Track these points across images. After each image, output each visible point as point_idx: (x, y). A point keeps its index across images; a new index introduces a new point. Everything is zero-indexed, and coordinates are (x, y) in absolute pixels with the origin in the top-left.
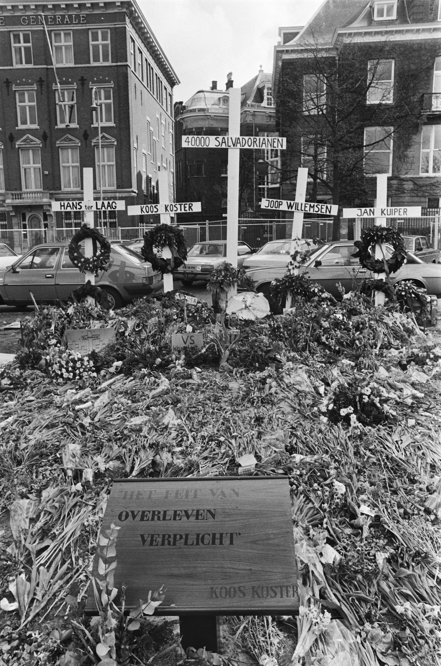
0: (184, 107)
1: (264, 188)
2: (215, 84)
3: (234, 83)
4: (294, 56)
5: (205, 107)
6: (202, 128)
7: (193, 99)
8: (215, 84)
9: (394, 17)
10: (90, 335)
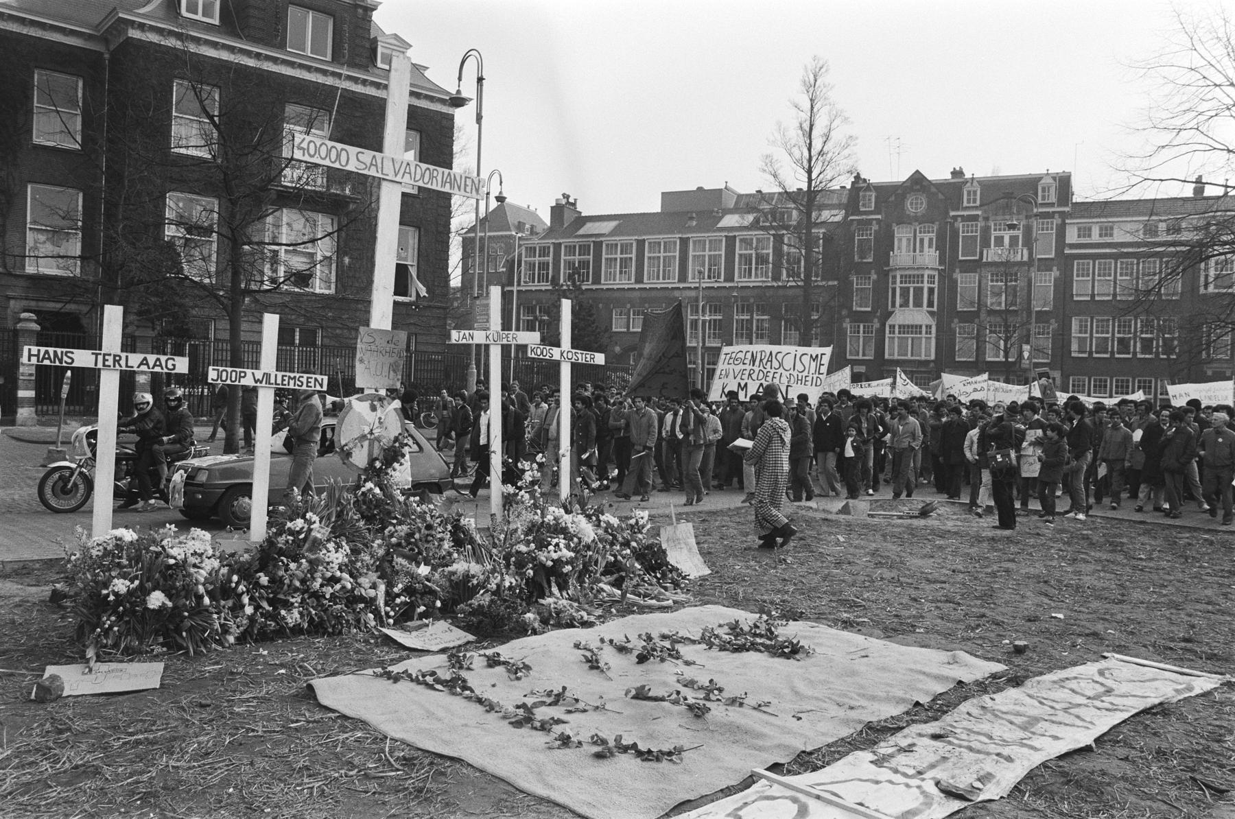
9: (216, 21)
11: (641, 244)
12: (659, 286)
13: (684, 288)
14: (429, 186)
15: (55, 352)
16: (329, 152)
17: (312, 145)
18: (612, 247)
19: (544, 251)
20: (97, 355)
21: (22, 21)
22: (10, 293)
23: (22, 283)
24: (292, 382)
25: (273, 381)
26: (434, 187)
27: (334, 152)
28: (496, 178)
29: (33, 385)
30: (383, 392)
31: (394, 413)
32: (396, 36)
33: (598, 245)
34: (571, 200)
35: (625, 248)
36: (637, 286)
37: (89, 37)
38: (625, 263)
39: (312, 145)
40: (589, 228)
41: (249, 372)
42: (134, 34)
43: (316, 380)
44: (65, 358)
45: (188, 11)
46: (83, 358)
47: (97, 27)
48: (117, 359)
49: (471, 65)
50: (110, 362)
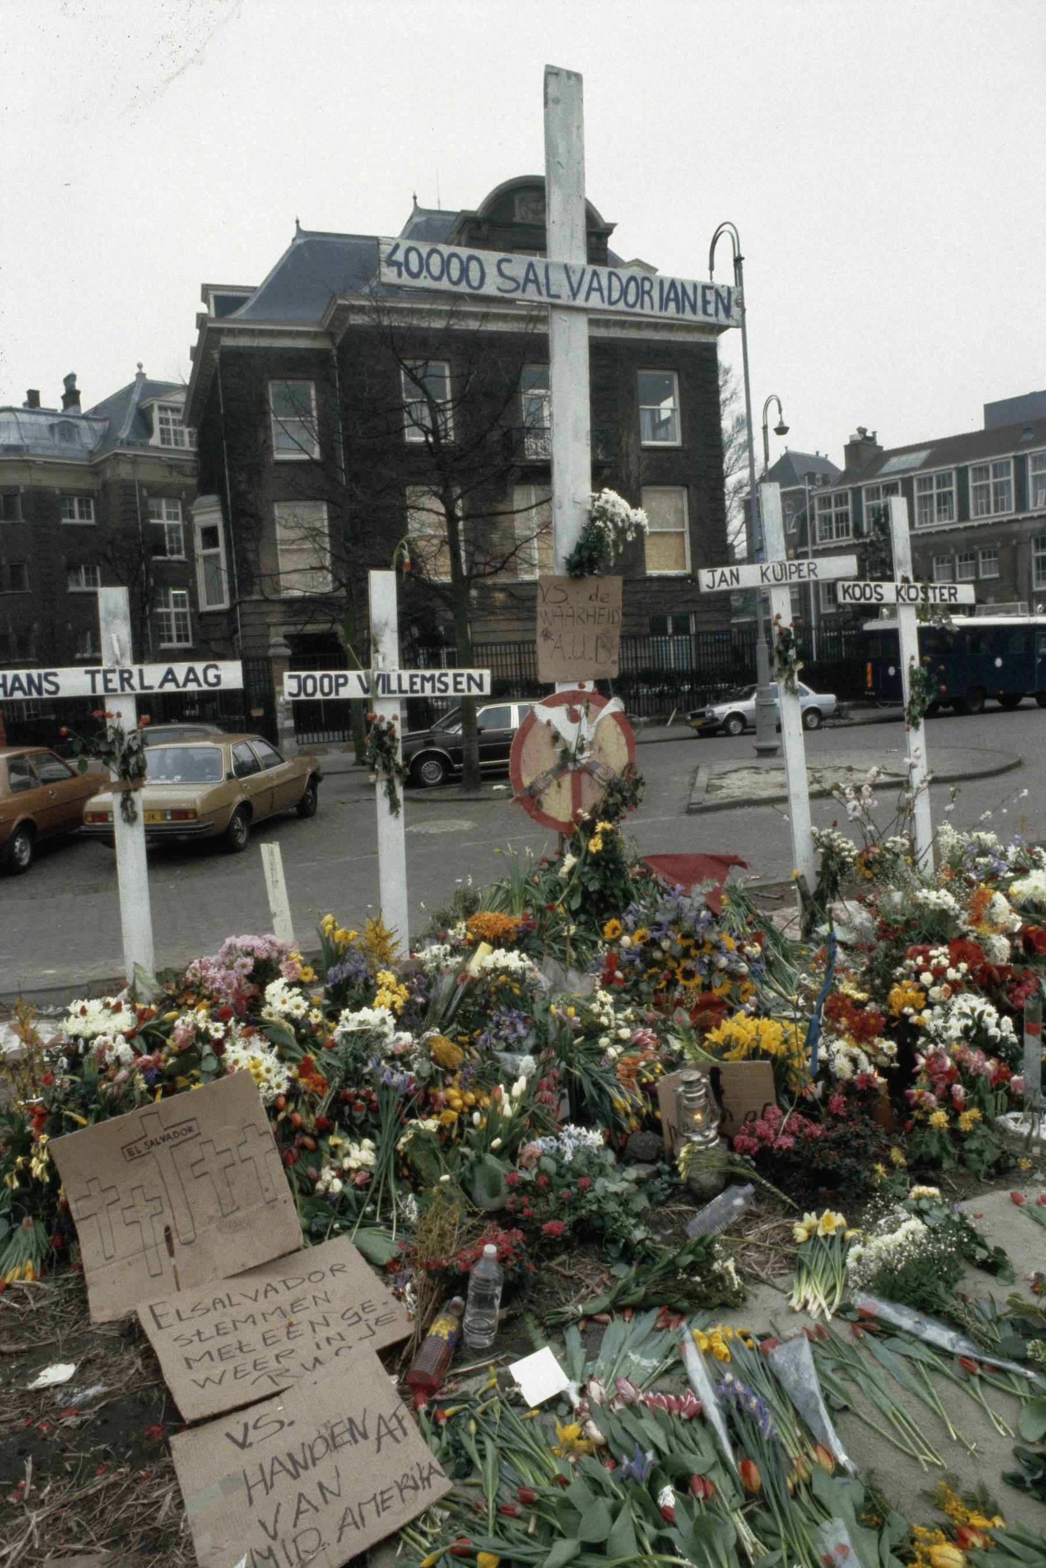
1: (168, 615)
2: (33, 396)
3: (82, 397)
4: (244, 342)
5: (20, 443)
6: (17, 487)
8: (33, 396)
11: (962, 473)
12: (990, 521)
13: (1024, 519)
14: (637, 309)
15: (29, 677)
16: (446, 265)
17: (413, 256)
18: (925, 483)
19: (841, 499)
20: (93, 673)
21: (252, 333)
24: (428, 686)
25: (394, 686)
26: (647, 310)
27: (455, 265)
28: (773, 406)
29: (290, 714)
30: (590, 687)
31: (612, 722)
32: (638, 263)
34: (869, 434)
35: (943, 480)
36: (961, 525)
37: (315, 335)
38: (944, 499)
39: (413, 256)
40: (895, 464)
41: (352, 675)
43: (470, 678)
44: (46, 685)
46: (72, 681)
47: (320, 323)
48: (125, 680)
49: (725, 242)
50: (115, 684)
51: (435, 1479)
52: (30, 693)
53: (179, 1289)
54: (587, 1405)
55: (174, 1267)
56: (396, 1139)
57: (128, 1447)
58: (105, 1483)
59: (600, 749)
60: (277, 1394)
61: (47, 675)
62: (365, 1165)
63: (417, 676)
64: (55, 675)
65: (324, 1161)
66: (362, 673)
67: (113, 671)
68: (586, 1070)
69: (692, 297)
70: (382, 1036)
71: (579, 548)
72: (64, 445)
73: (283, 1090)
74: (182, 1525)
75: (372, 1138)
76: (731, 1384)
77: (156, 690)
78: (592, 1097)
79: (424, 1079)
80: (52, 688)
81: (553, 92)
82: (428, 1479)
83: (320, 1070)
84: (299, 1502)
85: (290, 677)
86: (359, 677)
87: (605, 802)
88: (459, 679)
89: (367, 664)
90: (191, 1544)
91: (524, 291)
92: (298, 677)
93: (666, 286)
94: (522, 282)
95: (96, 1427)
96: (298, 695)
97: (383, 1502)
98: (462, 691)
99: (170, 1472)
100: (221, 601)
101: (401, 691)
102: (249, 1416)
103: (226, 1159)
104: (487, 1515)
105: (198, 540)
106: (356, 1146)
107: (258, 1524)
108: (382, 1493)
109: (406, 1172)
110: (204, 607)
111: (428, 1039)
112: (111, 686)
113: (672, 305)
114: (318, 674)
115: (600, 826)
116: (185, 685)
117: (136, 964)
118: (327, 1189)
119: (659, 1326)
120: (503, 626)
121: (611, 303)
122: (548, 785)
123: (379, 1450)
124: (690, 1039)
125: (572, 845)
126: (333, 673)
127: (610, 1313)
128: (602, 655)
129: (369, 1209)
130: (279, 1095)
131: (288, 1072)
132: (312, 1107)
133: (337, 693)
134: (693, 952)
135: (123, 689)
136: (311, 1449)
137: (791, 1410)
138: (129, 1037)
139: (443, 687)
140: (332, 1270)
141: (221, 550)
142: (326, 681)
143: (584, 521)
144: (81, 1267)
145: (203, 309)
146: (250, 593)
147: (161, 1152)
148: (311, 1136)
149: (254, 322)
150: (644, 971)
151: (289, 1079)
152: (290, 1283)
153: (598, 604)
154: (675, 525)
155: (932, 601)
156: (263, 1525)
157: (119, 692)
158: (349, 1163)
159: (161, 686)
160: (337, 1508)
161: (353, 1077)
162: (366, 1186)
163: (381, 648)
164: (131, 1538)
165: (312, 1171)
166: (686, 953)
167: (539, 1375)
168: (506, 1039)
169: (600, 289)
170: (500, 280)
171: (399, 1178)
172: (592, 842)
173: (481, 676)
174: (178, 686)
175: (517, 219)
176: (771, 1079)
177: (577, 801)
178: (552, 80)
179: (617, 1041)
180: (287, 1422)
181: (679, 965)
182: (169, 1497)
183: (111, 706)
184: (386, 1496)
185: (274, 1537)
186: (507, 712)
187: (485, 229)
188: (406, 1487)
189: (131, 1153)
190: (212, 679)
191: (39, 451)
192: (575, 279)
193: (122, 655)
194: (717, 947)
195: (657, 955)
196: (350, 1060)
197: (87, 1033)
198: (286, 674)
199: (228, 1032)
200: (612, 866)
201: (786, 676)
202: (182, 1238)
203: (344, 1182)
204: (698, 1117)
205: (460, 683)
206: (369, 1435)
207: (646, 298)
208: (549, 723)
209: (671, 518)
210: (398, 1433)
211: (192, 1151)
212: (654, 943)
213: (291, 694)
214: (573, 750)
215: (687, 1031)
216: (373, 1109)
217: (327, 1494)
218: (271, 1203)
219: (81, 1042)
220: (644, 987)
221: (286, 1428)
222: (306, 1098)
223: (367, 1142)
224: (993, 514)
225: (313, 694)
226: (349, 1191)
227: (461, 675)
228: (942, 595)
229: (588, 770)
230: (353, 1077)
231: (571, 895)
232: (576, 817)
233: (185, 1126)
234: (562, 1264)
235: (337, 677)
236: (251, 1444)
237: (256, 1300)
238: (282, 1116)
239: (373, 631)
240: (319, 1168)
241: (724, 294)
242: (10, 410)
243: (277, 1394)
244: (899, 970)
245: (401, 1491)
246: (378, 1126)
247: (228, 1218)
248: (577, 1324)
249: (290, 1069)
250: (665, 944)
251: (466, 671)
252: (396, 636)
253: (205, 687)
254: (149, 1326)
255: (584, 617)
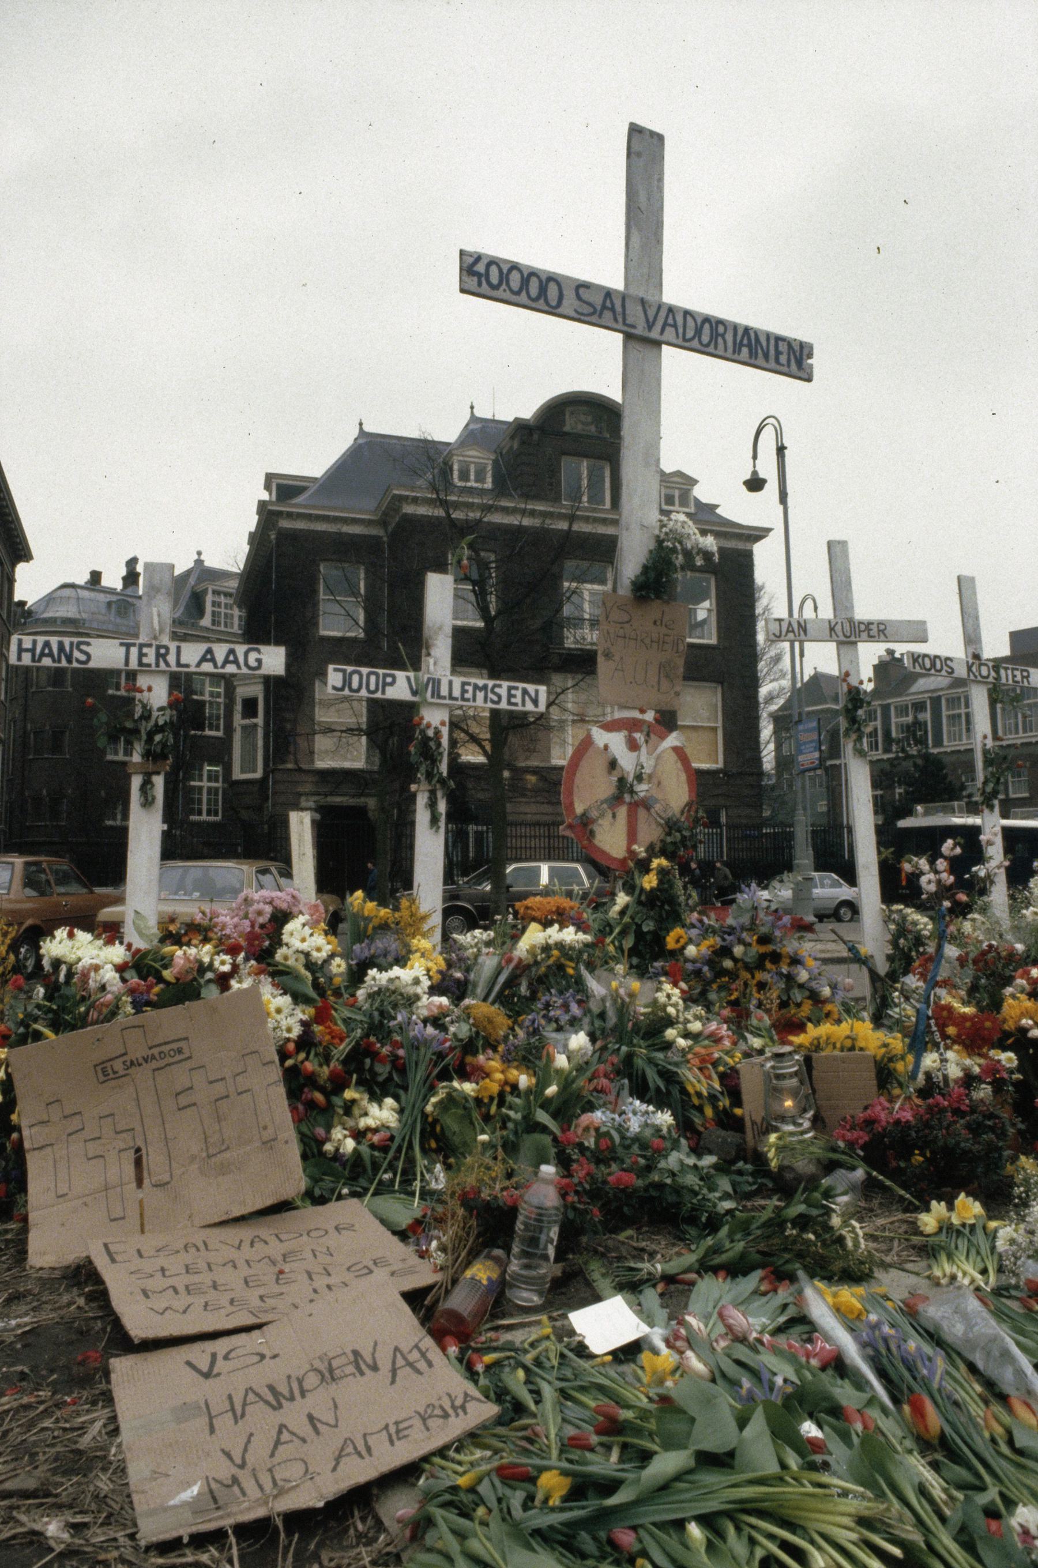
0: (30, 613)
1: (200, 788)
2: (96, 577)
4: (300, 525)
7: (49, 599)
8: (96, 577)
9: (488, 484)
10: (138, 1052)
15: (61, 645)
20: (128, 646)
21: (309, 517)
22: (300, 789)
23: (311, 778)
24: (480, 695)
25: (444, 691)
28: (809, 604)
30: (650, 716)
33: (936, 701)
34: (897, 655)
41: (400, 675)
42: (409, 509)
43: (525, 692)
44: (77, 654)
45: (461, 479)
48: (161, 655)
50: (150, 658)
51: (471, 1406)
52: (59, 661)
53: (143, 1231)
54: (683, 1331)
55: (141, 1202)
56: (425, 1100)
57: (52, 1371)
58: (15, 1404)
59: (659, 783)
60: (259, 1326)
61: (80, 643)
62: (385, 1127)
63: (469, 684)
64: (88, 644)
65: (336, 1120)
66: (411, 674)
67: (150, 645)
68: (651, 1061)
69: (764, 344)
70: (411, 1001)
71: (646, 569)
72: (119, 620)
73: (295, 1034)
74: (113, 1450)
75: (397, 1098)
76: (876, 1326)
77: (193, 669)
78: (658, 1089)
79: (461, 1040)
80: (83, 658)
81: (636, 148)
82: (463, 1407)
83: (339, 1022)
84: (280, 1432)
85: (336, 670)
86: (408, 679)
87: (662, 841)
88: (513, 692)
89: (416, 666)
90: (124, 1470)
91: (600, 316)
92: (344, 671)
93: (740, 333)
94: (599, 308)
95: (13, 1349)
96: (342, 689)
97: (398, 1432)
98: (516, 704)
99: (108, 1398)
100: (254, 771)
101: (451, 698)
102: (221, 1346)
103: (219, 1089)
104: (548, 1447)
105: (239, 707)
106: (375, 1105)
107: (220, 1453)
108: (397, 1423)
109: (433, 1145)
110: (237, 775)
111: (468, 1007)
112: (145, 660)
113: (745, 350)
114: (365, 670)
115: (655, 863)
116: (223, 667)
117: (136, 912)
118: (337, 1149)
119: (763, 1288)
120: (533, 808)
121: (685, 340)
122: (602, 815)
123: (393, 1382)
124: (772, 1039)
125: (624, 885)
126: (381, 671)
127: (698, 1273)
128: (665, 684)
129: (387, 1176)
130: (288, 1040)
131: (303, 1013)
132: (327, 1059)
133: (383, 692)
134: (768, 965)
135: (157, 665)
136: (300, 1382)
137: (962, 1367)
138: (120, 969)
139: (495, 698)
140: (337, 1228)
141: (260, 720)
142: (373, 678)
143: (652, 545)
144: (25, 1219)
145: (265, 496)
146: (284, 762)
147: (142, 1075)
148: (322, 1090)
149: (313, 507)
150: (713, 981)
151: (303, 1023)
152: (283, 1237)
153: (664, 630)
154: (709, 720)
155: (1004, 681)
156: (228, 1455)
157: (153, 668)
158: (363, 1122)
159: (198, 665)
160: (333, 1440)
161: (379, 1026)
162: (384, 1149)
163: (433, 653)
164: (41, 1458)
165: (320, 1131)
166: (760, 964)
167: (606, 1323)
168: (557, 1021)
169: (675, 326)
170: (577, 303)
171: (425, 1151)
172: (646, 878)
173: (537, 692)
174: (216, 666)
175: (567, 428)
176: (873, 1075)
177: (632, 836)
178: (636, 136)
179: (687, 1035)
180: (268, 1354)
181: (753, 977)
182: (98, 1425)
183: (142, 681)
184: (401, 1426)
185: (242, 1466)
186: (537, 872)
187: (536, 437)
188: (430, 1417)
189: (104, 1071)
190: (252, 662)
191: (95, 625)
192: (651, 313)
193: (161, 631)
194: (796, 961)
195: (728, 964)
196: (376, 1014)
197: (71, 957)
198: (331, 667)
199: (235, 968)
200: (667, 907)
201: (854, 736)
202: (154, 1179)
203: (358, 1143)
204: (789, 1103)
205: (514, 696)
206: (380, 1364)
207: (720, 340)
208: (606, 747)
209: (705, 714)
210: (422, 1365)
211: (180, 1076)
212: (725, 951)
213: (334, 688)
214: (630, 778)
215: (768, 1031)
216: (400, 1067)
217: (319, 1425)
218: (268, 1144)
219: (64, 969)
220: (713, 996)
221: (267, 1360)
222: (321, 1049)
223: (389, 1101)
224: (1021, 734)
225: (358, 690)
226: (364, 1149)
227: (516, 688)
228: (1014, 676)
229: (646, 804)
230: (379, 1026)
231: (623, 933)
232: (632, 853)
233: (174, 1046)
234: (631, 1238)
235: (385, 676)
236: (218, 1375)
237: (239, 1248)
238: (289, 1062)
239: (426, 632)
240: (329, 1128)
241: (797, 348)
242: (73, 586)
243: (259, 1326)
244: (1009, 990)
245: (424, 1420)
246: (406, 1089)
247: (213, 1159)
248: (654, 1286)
249: (304, 1012)
250: (738, 950)
251: (521, 685)
252: (449, 641)
253: (245, 670)
254: (101, 1263)
255: (648, 641)
